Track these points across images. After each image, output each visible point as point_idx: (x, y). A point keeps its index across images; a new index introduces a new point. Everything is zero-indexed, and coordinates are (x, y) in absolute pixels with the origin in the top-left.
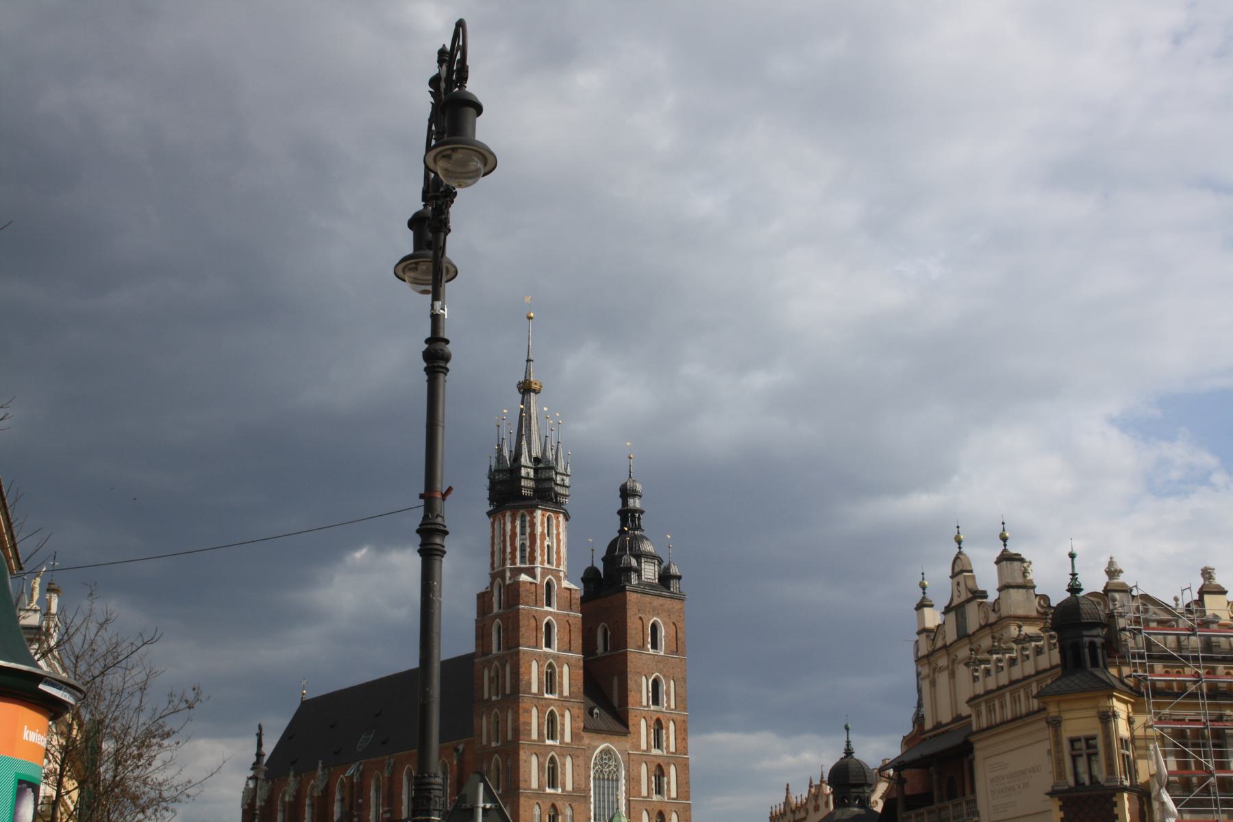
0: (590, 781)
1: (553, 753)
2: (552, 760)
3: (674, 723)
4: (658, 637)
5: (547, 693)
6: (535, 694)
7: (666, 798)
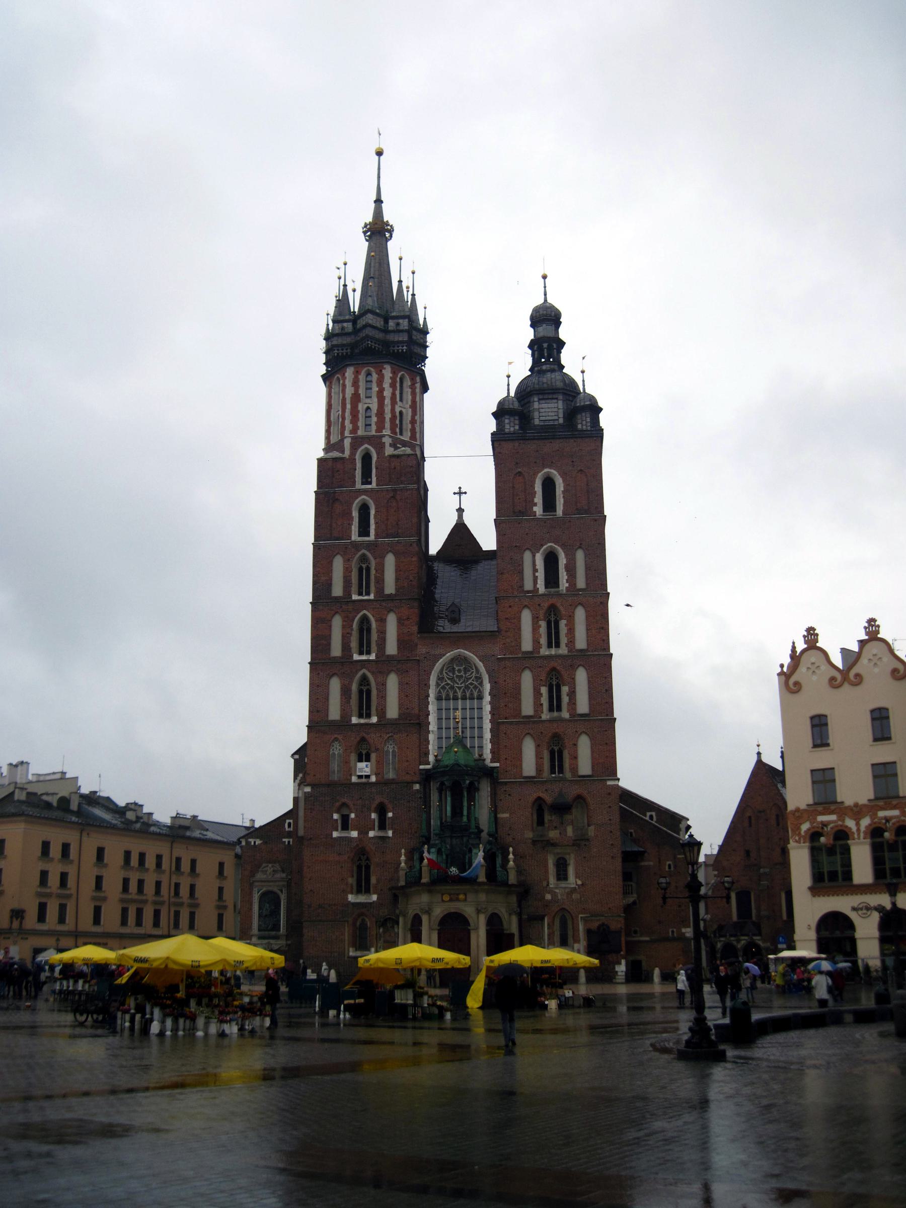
0: (429, 703)
1: (364, 671)
2: (364, 680)
3: (584, 607)
4: (557, 494)
5: (360, 594)
6: (336, 598)
7: (565, 714)
